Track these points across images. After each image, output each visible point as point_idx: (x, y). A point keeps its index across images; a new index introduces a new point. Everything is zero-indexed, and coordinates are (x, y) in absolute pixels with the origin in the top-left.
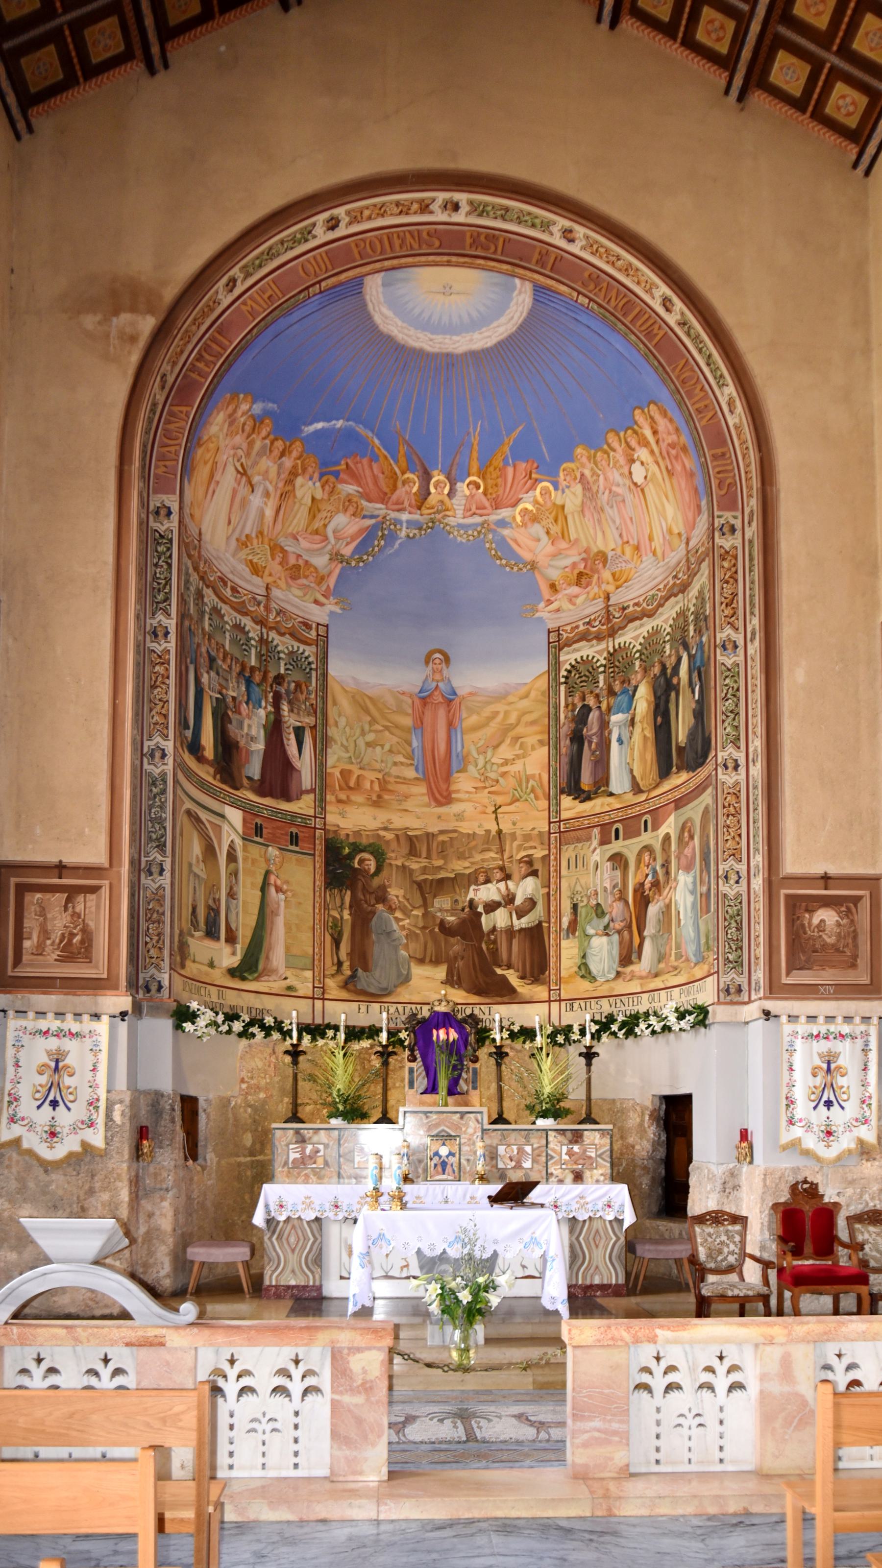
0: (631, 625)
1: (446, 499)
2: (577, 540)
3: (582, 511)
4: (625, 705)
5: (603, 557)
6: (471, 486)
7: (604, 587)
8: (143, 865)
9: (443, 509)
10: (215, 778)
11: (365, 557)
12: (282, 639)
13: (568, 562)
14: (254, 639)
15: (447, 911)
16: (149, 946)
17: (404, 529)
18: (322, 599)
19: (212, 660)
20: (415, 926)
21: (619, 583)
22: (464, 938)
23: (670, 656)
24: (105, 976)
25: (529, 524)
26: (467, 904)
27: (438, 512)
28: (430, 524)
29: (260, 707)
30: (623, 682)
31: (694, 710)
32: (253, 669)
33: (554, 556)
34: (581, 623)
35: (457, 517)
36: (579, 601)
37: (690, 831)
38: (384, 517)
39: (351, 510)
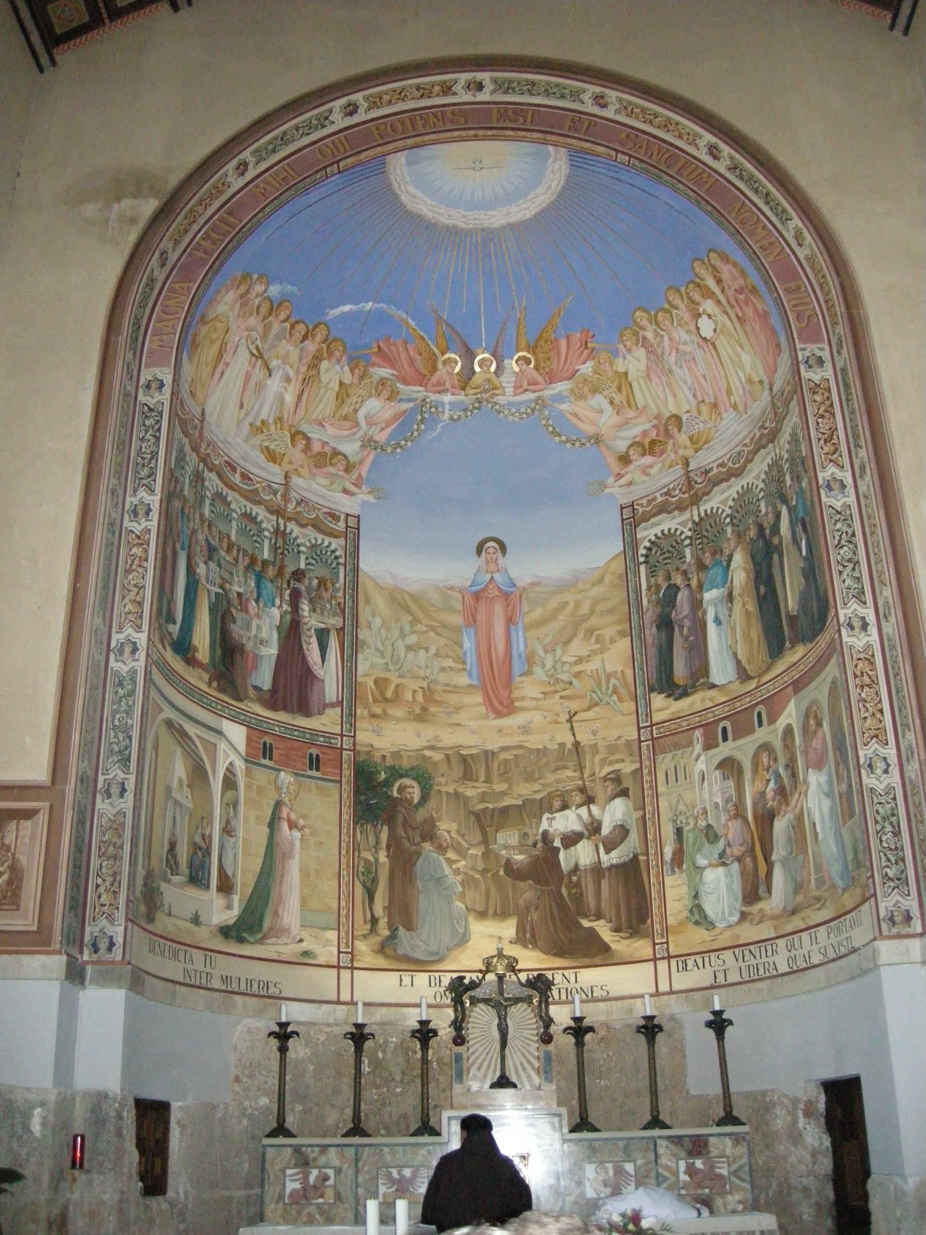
0: (716, 489)
1: (494, 378)
2: (645, 408)
3: (648, 376)
4: (719, 579)
5: (677, 419)
6: (520, 362)
7: (681, 452)
8: (100, 785)
9: (492, 388)
10: (210, 686)
11: (403, 443)
12: (303, 530)
13: (637, 431)
14: (269, 530)
15: (513, 848)
16: (102, 889)
17: (447, 411)
18: (353, 489)
19: (211, 552)
20: (473, 869)
21: (698, 446)
22: (538, 882)
23: (766, 514)
24: (35, 928)
25: (589, 396)
26: (539, 837)
27: (485, 391)
28: (477, 405)
29: (274, 605)
30: (714, 553)
31: (803, 569)
32: (265, 563)
33: (621, 426)
34: (658, 494)
35: (507, 397)
36: (654, 470)
37: (816, 717)
38: (424, 400)
39: (386, 394)
